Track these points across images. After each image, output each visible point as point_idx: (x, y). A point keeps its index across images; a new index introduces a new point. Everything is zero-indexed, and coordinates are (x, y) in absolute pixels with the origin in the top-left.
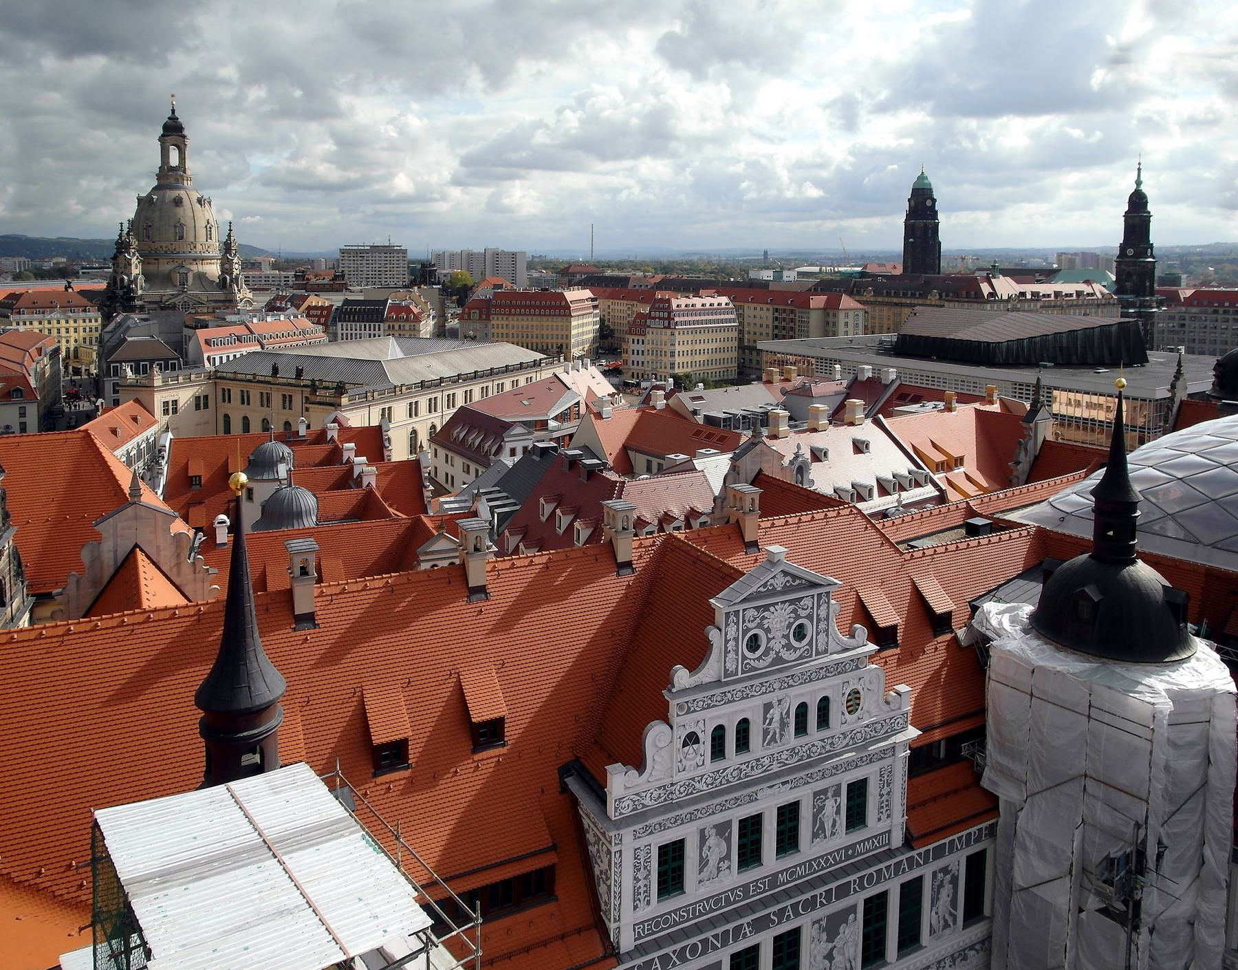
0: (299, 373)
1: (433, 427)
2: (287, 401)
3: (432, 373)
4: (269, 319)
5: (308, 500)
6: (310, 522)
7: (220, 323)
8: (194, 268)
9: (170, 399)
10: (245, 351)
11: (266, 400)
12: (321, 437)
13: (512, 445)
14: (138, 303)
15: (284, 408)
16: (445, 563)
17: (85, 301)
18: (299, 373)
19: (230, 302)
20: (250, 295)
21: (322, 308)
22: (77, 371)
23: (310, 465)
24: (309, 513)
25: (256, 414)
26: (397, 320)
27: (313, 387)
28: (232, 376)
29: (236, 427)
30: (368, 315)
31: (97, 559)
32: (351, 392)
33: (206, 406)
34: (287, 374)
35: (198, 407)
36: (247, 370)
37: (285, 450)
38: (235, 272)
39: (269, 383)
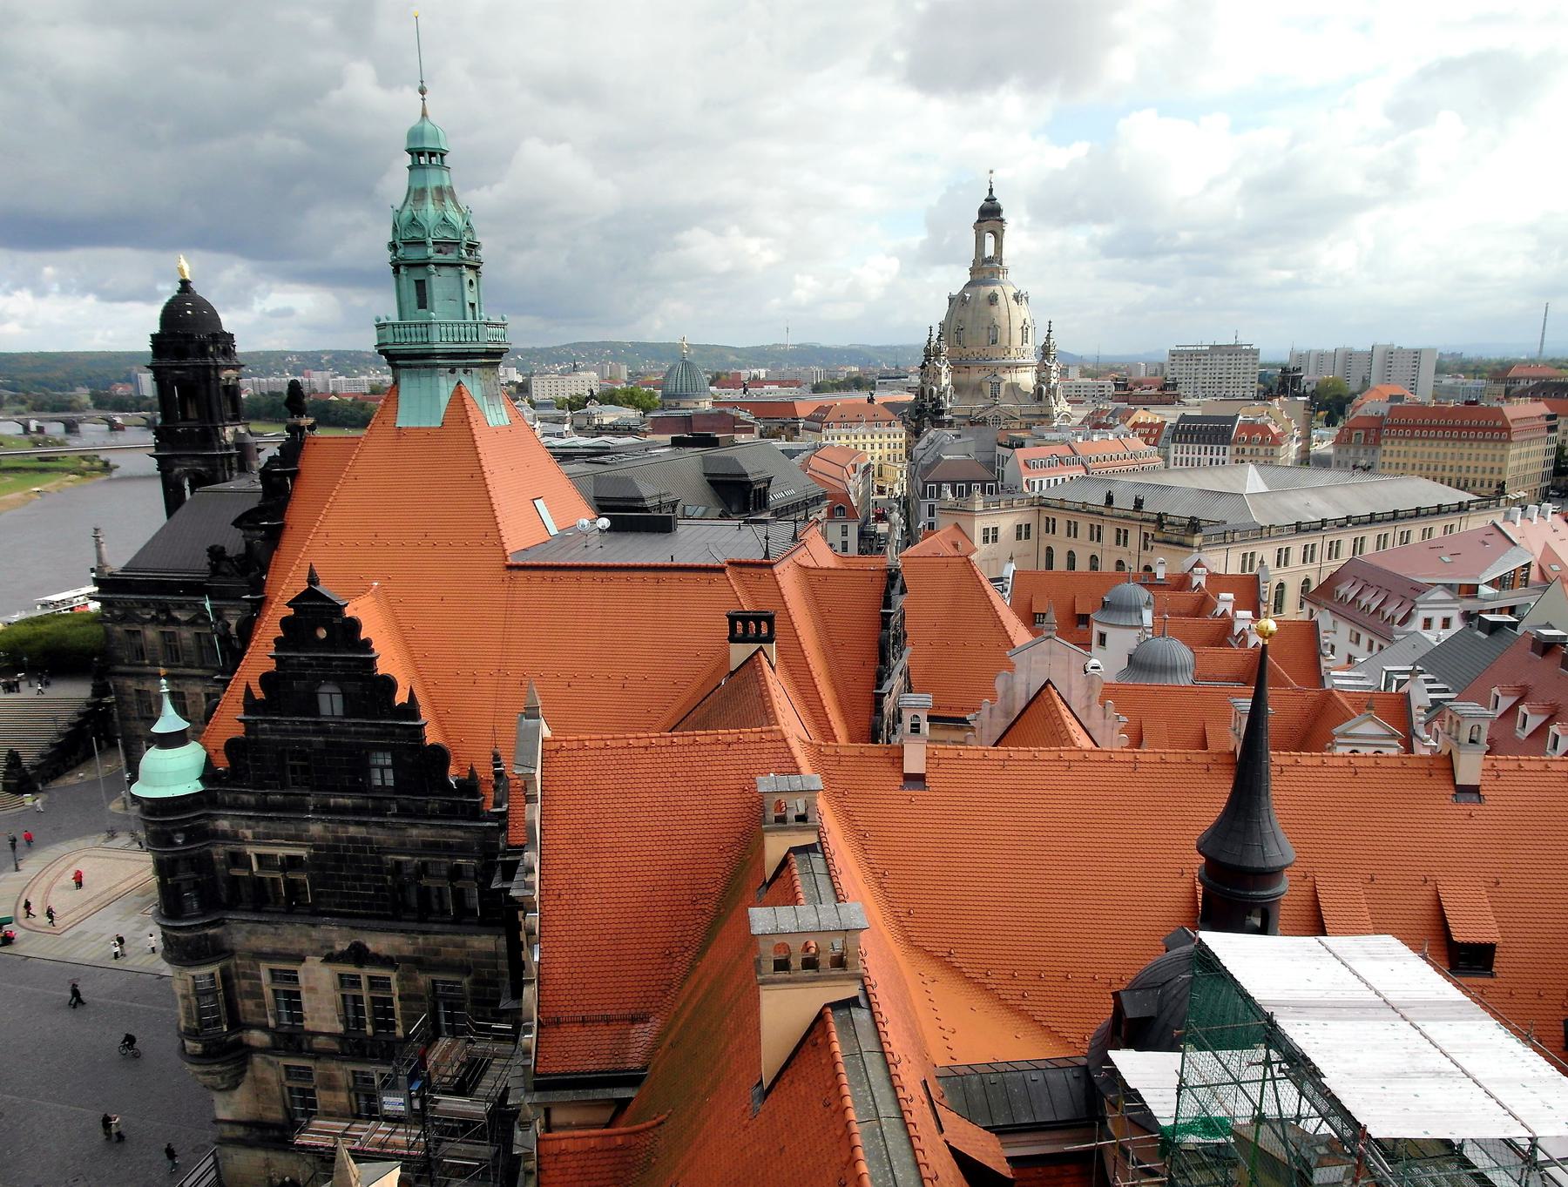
0: (1139, 504)
1: (1307, 581)
2: (1122, 537)
3: (1311, 513)
4: (1096, 438)
5: (1182, 653)
6: (1185, 680)
7: (1039, 441)
8: (1008, 378)
9: (991, 526)
10: (1067, 474)
11: (1096, 534)
12: (1183, 582)
13: (1428, 614)
14: (947, 417)
15: (1118, 543)
16: (1370, 751)
17: (890, 415)
18: (1139, 504)
19: (1045, 417)
20: (1069, 409)
21: (1152, 426)
22: (881, 491)
23: (1180, 615)
24: (1184, 669)
25: (1084, 549)
26: (1249, 442)
27: (1160, 521)
28: (1059, 504)
29: (1060, 563)
30: (1209, 433)
31: (1009, 689)
32: (1206, 531)
33: (1028, 536)
34: (1124, 502)
35: (1019, 536)
36: (1076, 496)
37: (1144, 594)
38: (1054, 381)
39: (1101, 514)
